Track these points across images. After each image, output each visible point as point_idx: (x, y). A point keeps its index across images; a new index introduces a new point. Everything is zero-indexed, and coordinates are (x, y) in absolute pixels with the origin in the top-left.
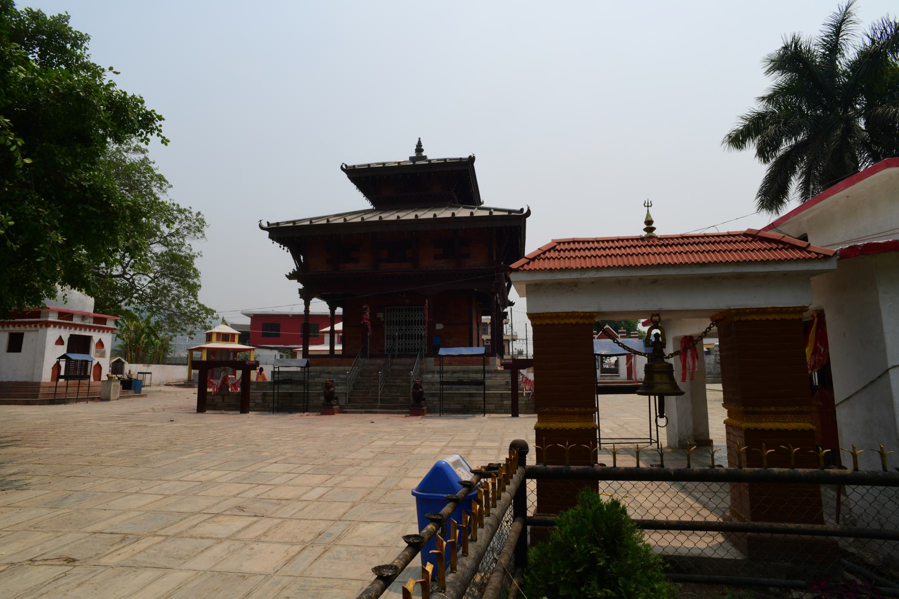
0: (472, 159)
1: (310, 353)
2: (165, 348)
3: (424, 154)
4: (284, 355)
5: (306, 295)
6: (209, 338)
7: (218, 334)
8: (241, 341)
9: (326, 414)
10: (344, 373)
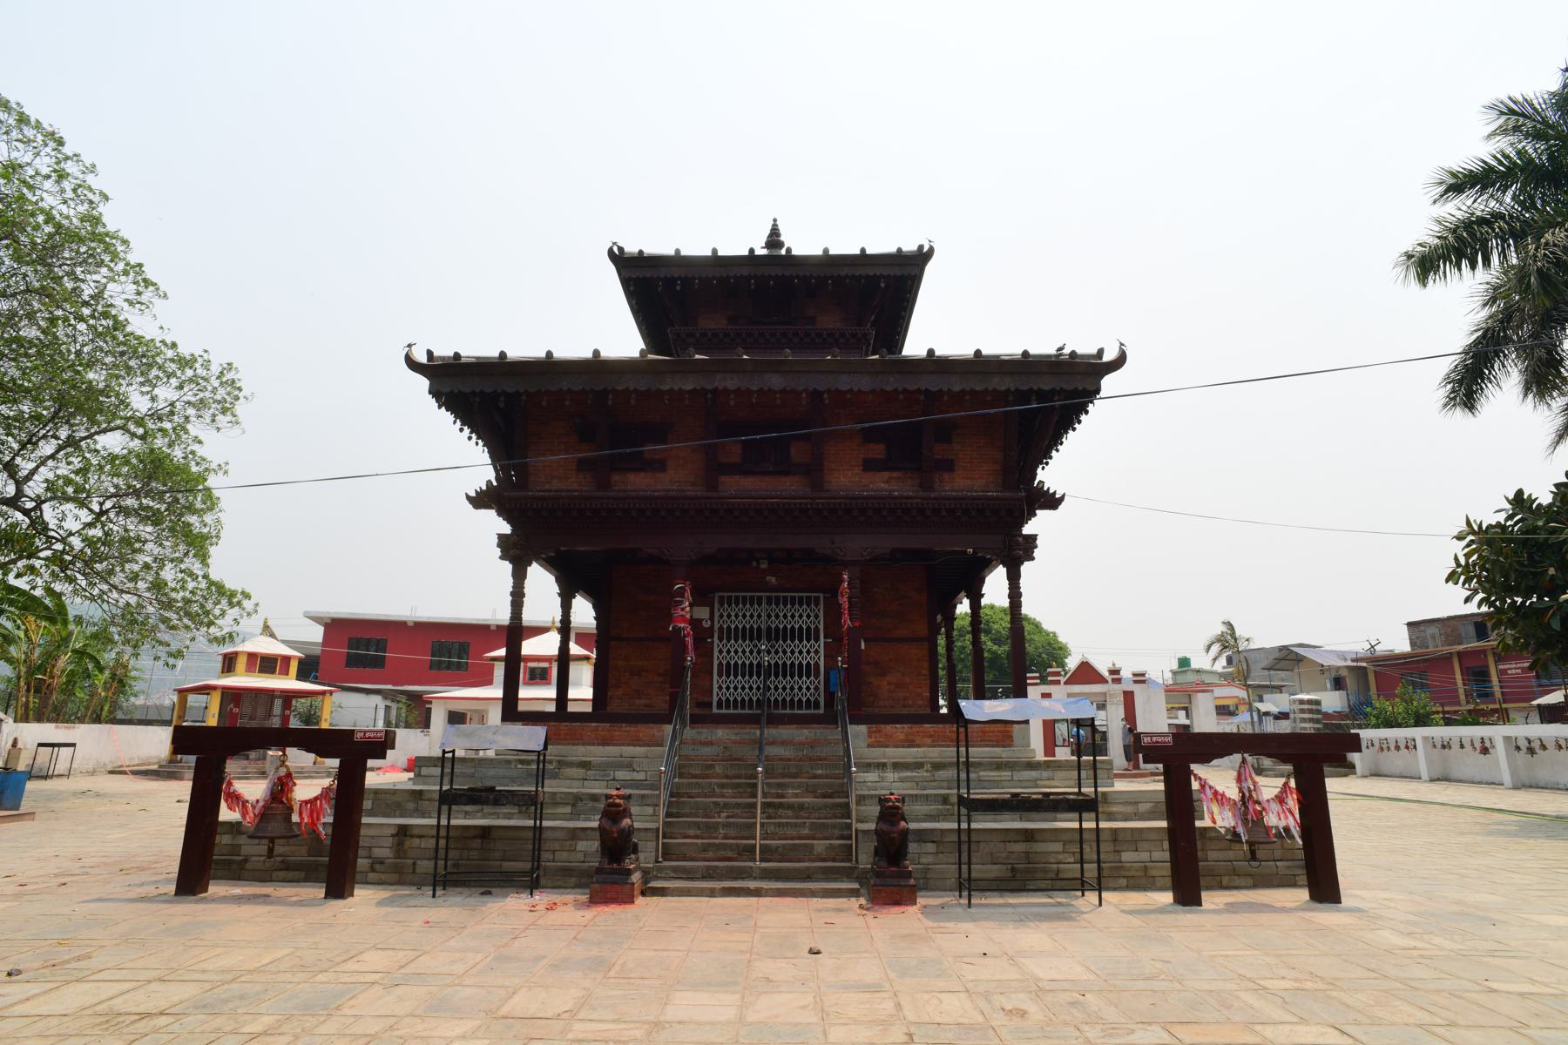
1: (522, 707)
2: (120, 682)
4: (394, 706)
5: (517, 552)
6: (229, 663)
8: (302, 676)
9: (607, 901)
10: (629, 766)
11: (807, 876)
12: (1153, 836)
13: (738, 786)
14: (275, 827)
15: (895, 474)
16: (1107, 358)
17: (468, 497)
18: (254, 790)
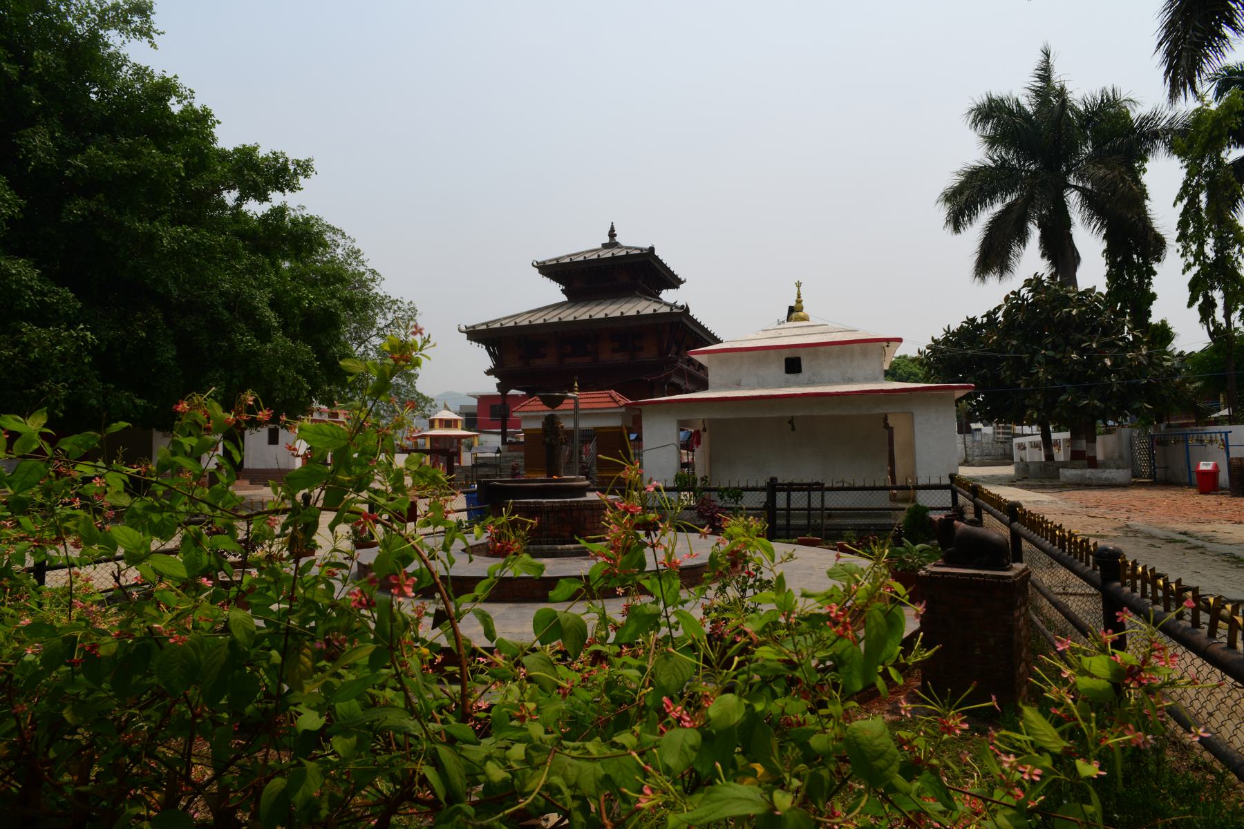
0: (652, 249)
3: (617, 239)
6: (432, 424)
7: (441, 420)
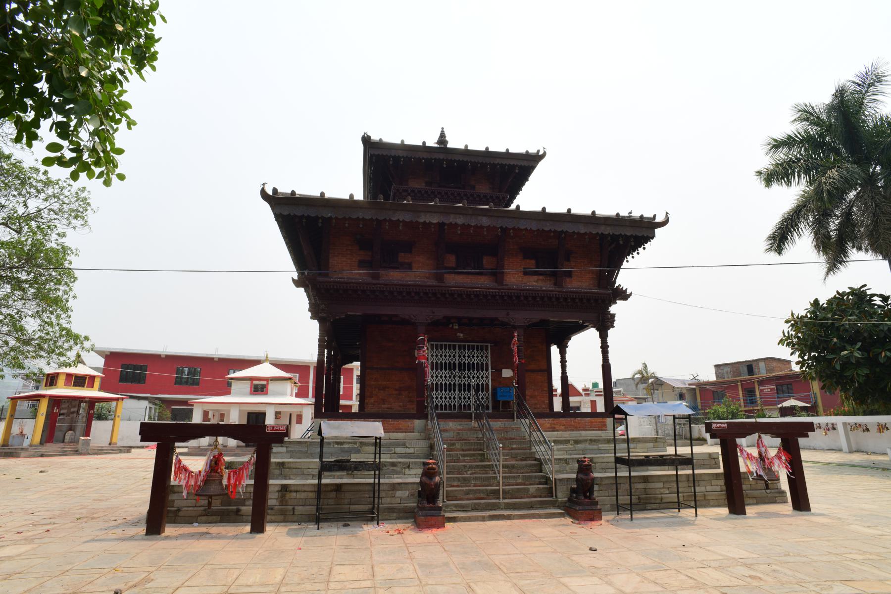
4: (153, 407)
8: (102, 388)
10: (404, 445)
11: (531, 506)
12: (707, 478)
13: (473, 455)
14: (213, 489)
15: (541, 277)
16: (658, 220)
17: (293, 280)
18: (197, 464)
